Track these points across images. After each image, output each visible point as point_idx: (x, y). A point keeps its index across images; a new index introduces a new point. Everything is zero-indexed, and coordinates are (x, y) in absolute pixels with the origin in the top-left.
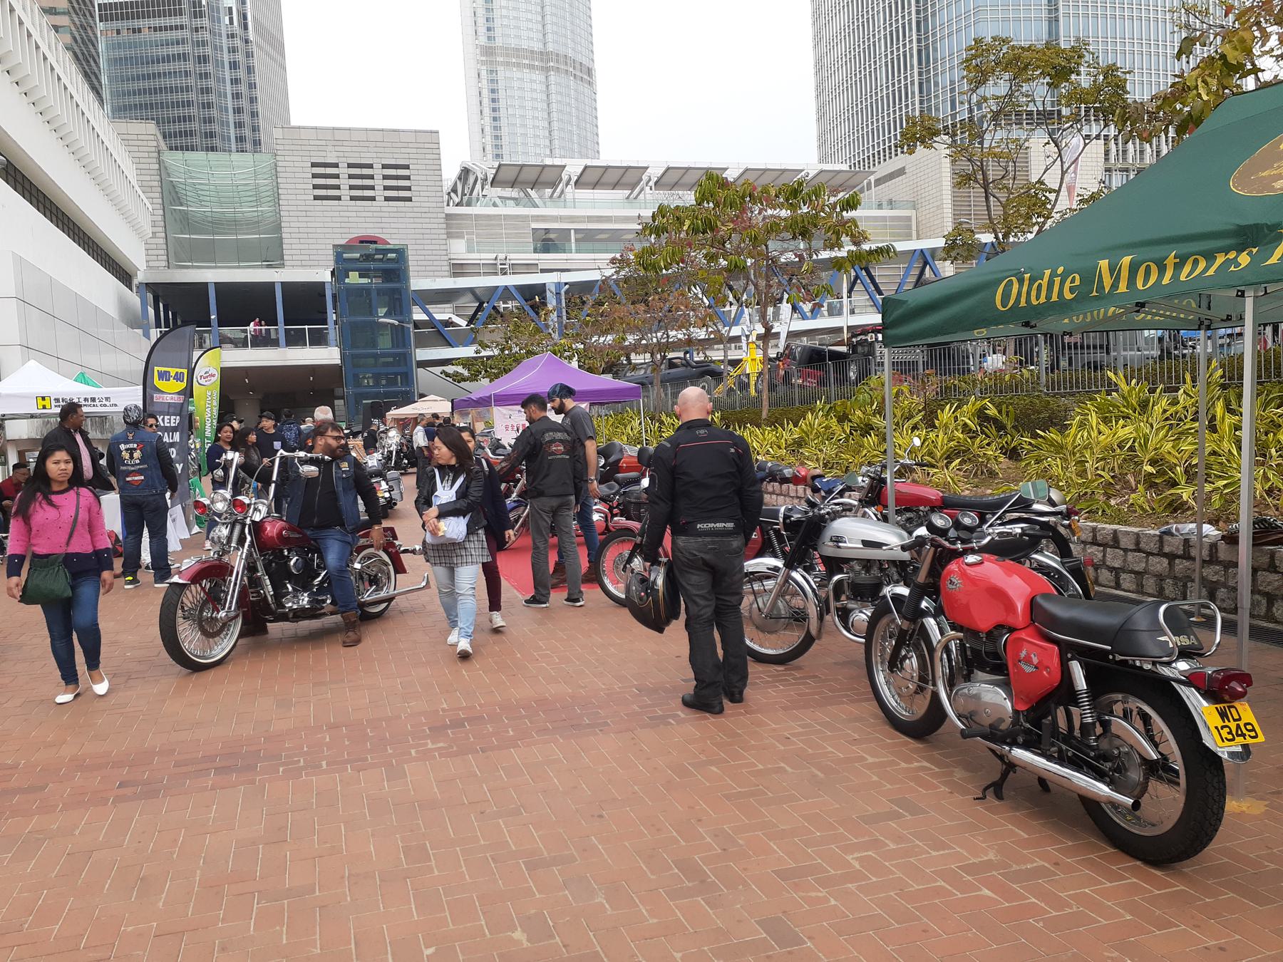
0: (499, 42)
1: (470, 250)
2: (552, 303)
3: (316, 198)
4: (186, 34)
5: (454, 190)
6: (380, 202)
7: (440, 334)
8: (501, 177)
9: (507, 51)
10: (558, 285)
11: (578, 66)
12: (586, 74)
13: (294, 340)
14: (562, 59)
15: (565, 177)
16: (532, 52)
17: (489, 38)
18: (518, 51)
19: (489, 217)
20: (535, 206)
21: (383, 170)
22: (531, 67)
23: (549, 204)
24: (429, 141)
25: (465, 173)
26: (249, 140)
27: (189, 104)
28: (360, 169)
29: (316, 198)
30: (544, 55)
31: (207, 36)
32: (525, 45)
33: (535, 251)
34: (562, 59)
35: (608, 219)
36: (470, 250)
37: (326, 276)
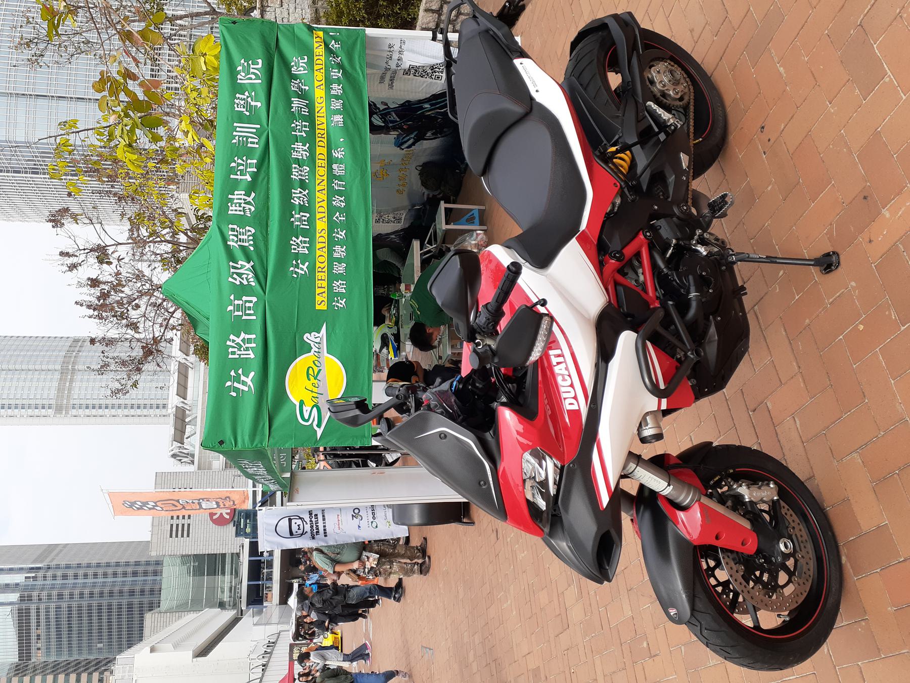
0: (53, 402)
3: (188, 536)
4: (42, 606)
9: (59, 396)
11: (72, 349)
14: (67, 360)
15: (180, 405)
17: (49, 408)
18: (60, 390)
22: (71, 381)
26: (155, 568)
27: (90, 606)
29: (188, 536)
30: (63, 372)
34: (67, 360)
37: (248, 540)
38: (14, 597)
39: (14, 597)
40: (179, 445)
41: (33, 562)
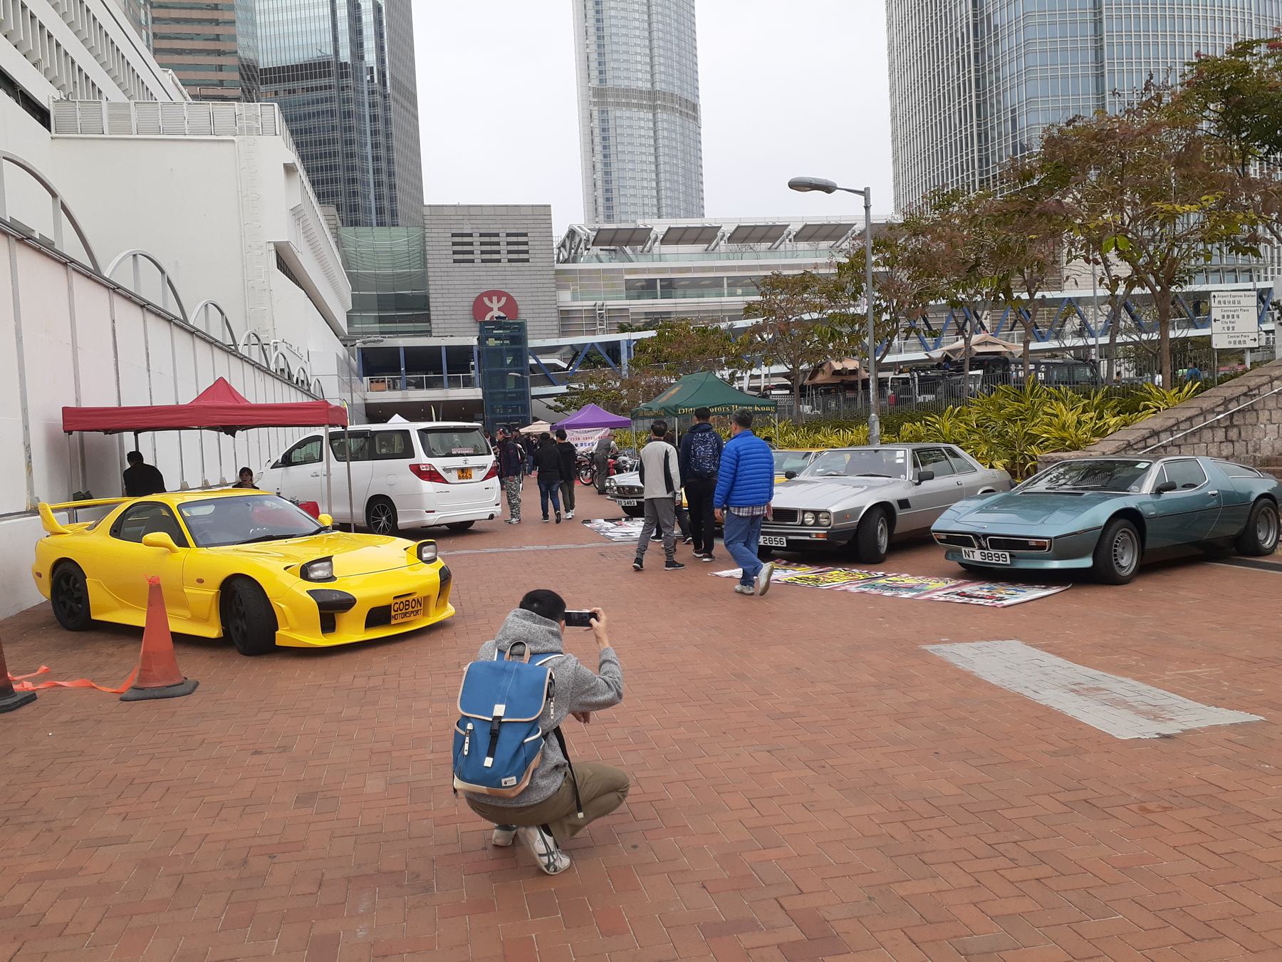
0: (610, 84)
1: (574, 299)
2: (624, 358)
3: (455, 261)
4: (334, 92)
5: (563, 245)
6: (504, 264)
7: (549, 375)
8: (599, 239)
9: (618, 92)
10: (629, 341)
11: (683, 103)
12: (690, 110)
13: (454, 383)
15: (652, 236)
16: (641, 92)
17: (601, 81)
18: (627, 92)
19: (590, 271)
20: (631, 261)
21: (504, 236)
22: (640, 106)
23: (641, 257)
24: (542, 214)
25: (572, 233)
28: (489, 238)
29: (455, 261)
30: (652, 94)
31: (351, 94)
32: (634, 85)
33: (628, 298)
35: (688, 270)
36: (574, 299)
38: (345, 55)
39: (345, 55)
40: (592, 239)
41: (391, 74)
